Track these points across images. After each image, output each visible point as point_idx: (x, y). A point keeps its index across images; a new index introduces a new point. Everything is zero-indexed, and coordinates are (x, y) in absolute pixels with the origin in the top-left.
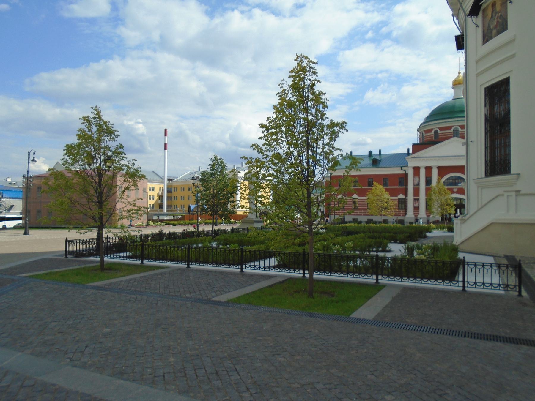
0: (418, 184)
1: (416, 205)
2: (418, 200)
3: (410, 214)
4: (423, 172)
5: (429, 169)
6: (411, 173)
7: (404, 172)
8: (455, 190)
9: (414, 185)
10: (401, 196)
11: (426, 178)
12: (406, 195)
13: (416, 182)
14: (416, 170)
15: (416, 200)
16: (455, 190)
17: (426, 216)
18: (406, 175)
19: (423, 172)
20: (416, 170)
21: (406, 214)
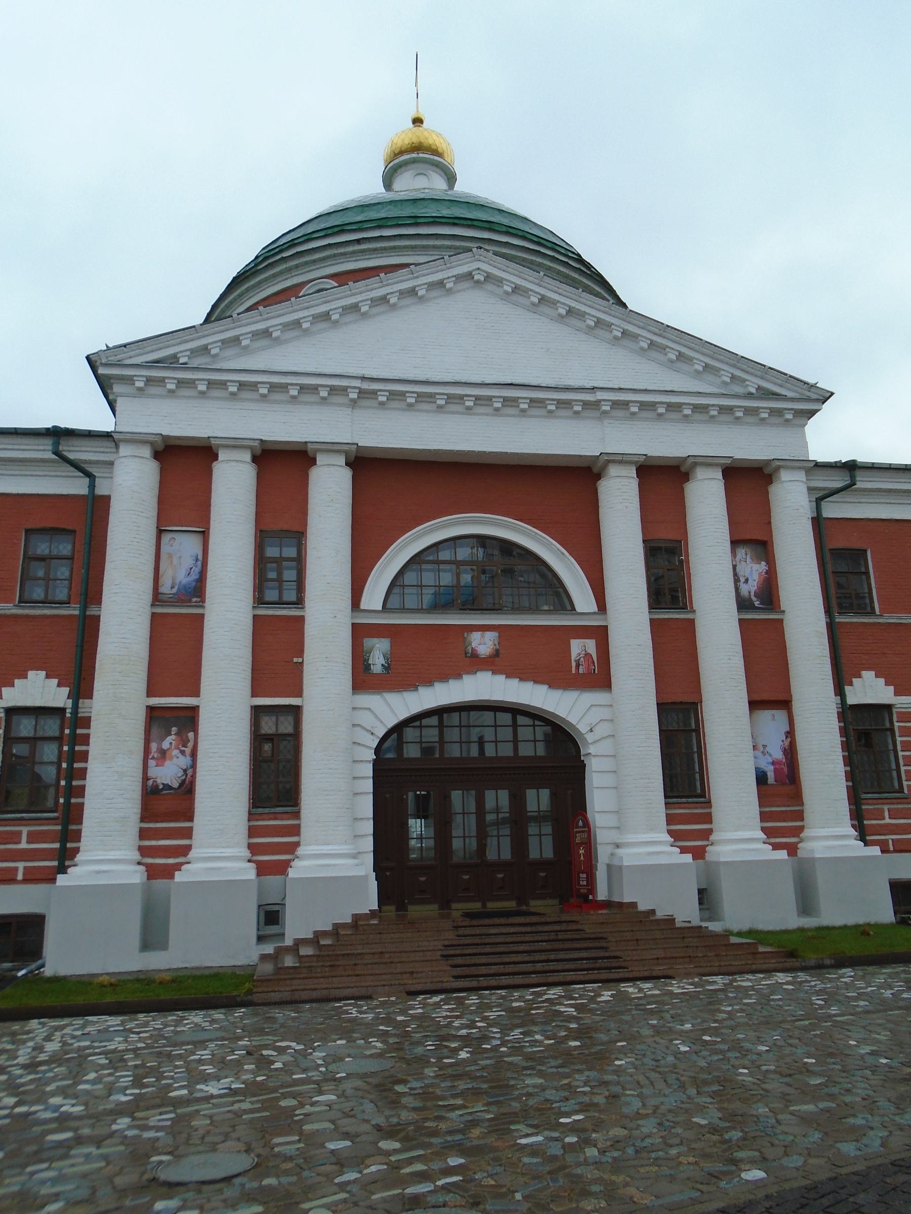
0: (197, 590)
1: (168, 773)
2: (187, 720)
3: (108, 852)
4: (233, 488)
5: (283, 467)
6: (132, 486)
7: (77, 486)
8: (483, 644)
9: (157, 598)
10: (38, 689)
11: (262, 537)
12: (81, 683)
13: (177, 574)
14: (184, 464)
15: (173, 722)
16: (483, 644)
17: (249, 873)
18: (97, 508)
19: (233, 488)
20: (184, 464)
21: (65, 857)
